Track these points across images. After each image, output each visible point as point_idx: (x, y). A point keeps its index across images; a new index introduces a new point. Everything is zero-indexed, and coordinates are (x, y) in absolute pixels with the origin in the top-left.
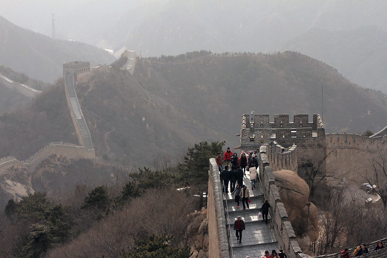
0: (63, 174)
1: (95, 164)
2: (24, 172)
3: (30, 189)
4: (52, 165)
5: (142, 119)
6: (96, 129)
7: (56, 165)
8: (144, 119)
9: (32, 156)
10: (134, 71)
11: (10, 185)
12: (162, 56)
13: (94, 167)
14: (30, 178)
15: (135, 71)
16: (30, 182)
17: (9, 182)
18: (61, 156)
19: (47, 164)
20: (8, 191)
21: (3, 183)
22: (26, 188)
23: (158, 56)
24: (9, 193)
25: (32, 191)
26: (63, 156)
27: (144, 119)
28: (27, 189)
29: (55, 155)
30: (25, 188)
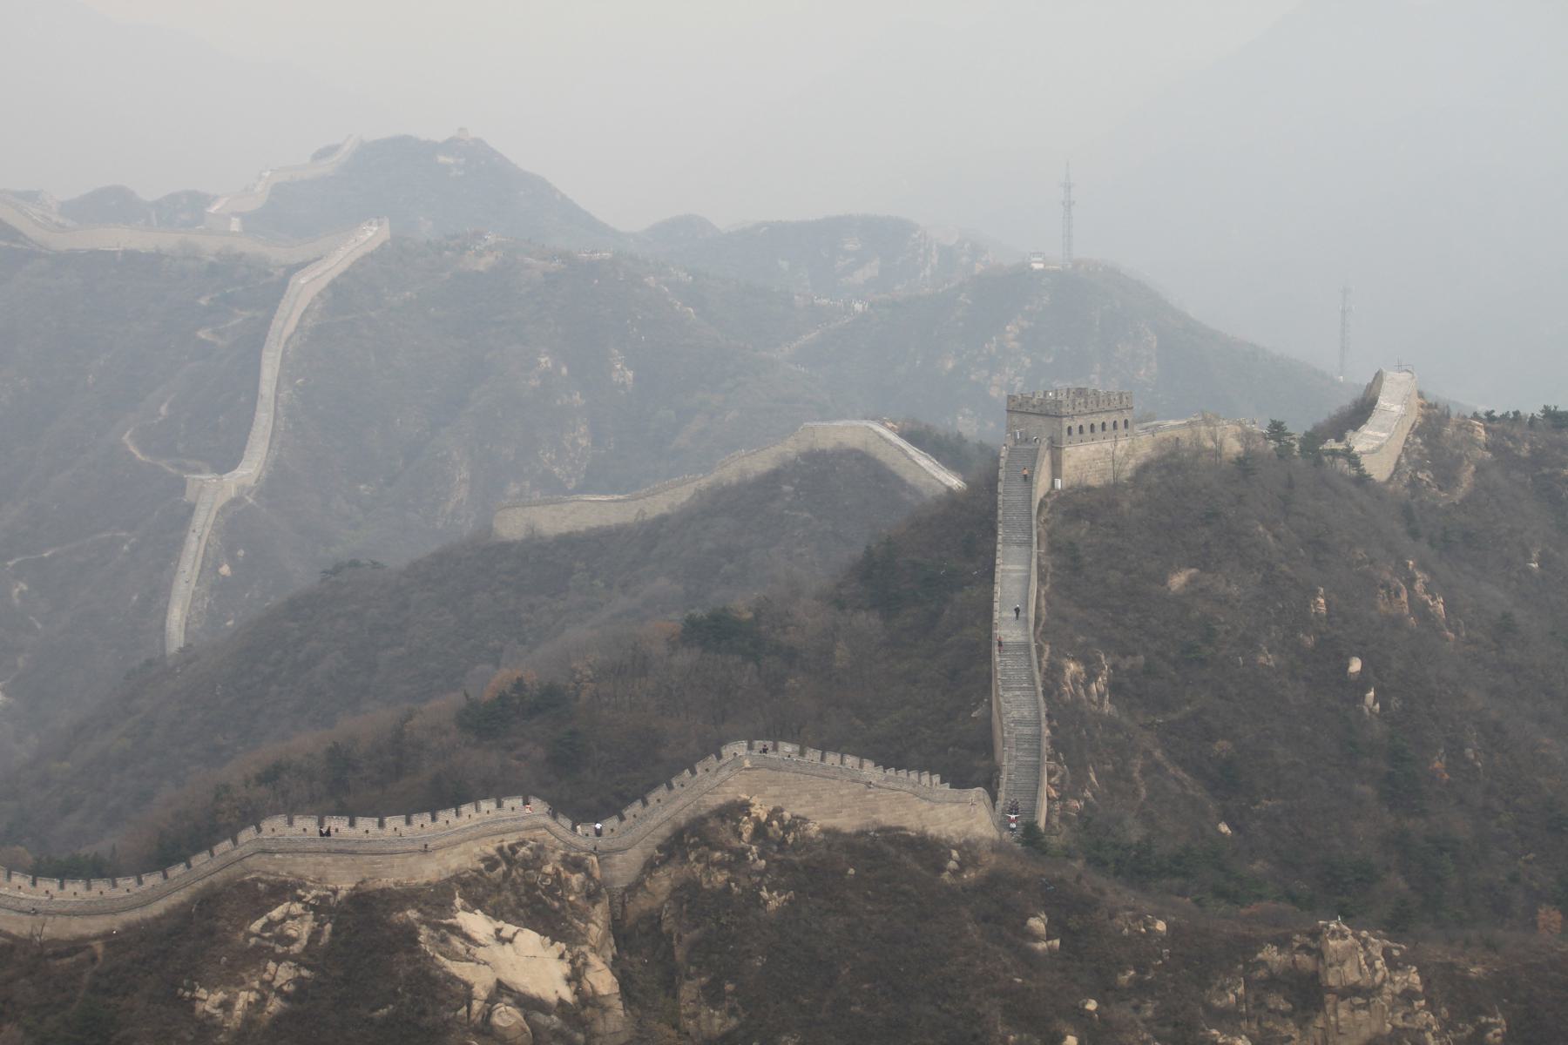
0: (766, 902)
1: (952, 865)
2: (567, 879)
3: (586, 964)
4: (718, 855)
5: (1348, 665)
6: (1101, 696)
7: (741, 854)
8: (1356, 666)
9: (638, 803)
10: (1398, 463)
11: (476, 936)
12: (1546, 410)
13: (946, 876)
14: (600, 913)
15: (1400, 457)
16: (596, 931)
17: (477, 924)
18: (776, 813)
19: (695, 846)
20: (455, 968)
21: (436, 927)
22: (568, 956)
23: (1532, 408)
24: (453, 979)
26: (787, 815)
27: (1356, 666)
28: (572, 962)
29: (744, 807)
30: (562, 957)
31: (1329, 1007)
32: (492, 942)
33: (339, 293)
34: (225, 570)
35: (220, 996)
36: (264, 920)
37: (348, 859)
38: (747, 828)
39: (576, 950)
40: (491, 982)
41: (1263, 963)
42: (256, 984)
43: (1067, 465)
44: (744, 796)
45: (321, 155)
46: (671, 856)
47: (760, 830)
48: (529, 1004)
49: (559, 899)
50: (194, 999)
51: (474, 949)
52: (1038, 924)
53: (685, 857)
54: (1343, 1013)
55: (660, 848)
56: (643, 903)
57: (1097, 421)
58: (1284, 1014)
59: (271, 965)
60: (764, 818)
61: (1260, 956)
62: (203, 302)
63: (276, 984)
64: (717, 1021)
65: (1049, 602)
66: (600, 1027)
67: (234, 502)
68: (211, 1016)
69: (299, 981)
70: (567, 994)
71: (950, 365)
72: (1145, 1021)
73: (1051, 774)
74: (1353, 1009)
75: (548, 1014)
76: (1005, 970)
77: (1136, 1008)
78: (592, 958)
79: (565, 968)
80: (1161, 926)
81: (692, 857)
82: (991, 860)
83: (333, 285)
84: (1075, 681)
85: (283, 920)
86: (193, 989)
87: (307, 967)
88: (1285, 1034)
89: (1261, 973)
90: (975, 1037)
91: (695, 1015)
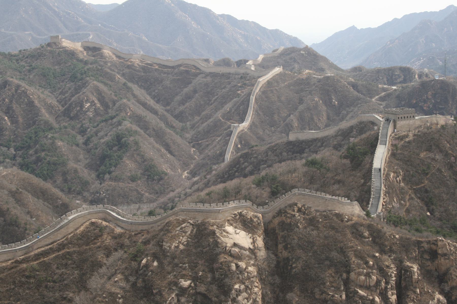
11: (230, 232)
17: (230, 229)
18: (304, 206)
22: (252, 237)
25: (260, 242)
26: (306, 206)
28: (253, 239)
29: (296, 204)
30: (250, 238)
31: (439, 259)
32: (234, 234)
33: (269, 83)
34: (239, 146)
35: (168, 244)
36: (180, 227)
37: (201, 213)
38: (296, 209)
39: (254, 236)
40: (233, 243)
41: (423, 247)
42: (177, 242)
43: (398, 126)
44: (296, 202)
45: (274, 51)
46: (278, 215)
48: (241, 248)
49: (251, 224)
50: (162, 245)
51: (229, 235)
53: (282, 215)
54: (442, 260)
55: (276, 213)
56: (272, 226)
57: (406, 116)
58: (427, 260)
59: (181, 238)
60: (300, 207)
61: (422, 245)
62: (239, 85)
63: (182, 242)
64: (286, 254)
65: (389, 158)
66: (258, 255)
67: (242, 130)
68: (166, 249)
70: (251, 247)
71: (414, 102)
72: (391, 259)
73: (384, 199)
74: (445, 259)
75: (246, 251)
76: (356, 245)
77: (390, 256)
78: (258, 238)
79: (251, 240)
81: (283, 215)
82: (355, 219)
83: (268, 81)
84: (393, 177)
85: (185, 227)
86: (162, 243)
87: (190, 238)
88: (428, 264)
89: (422, 249)
90: (347, 261)
91: (281, 253)
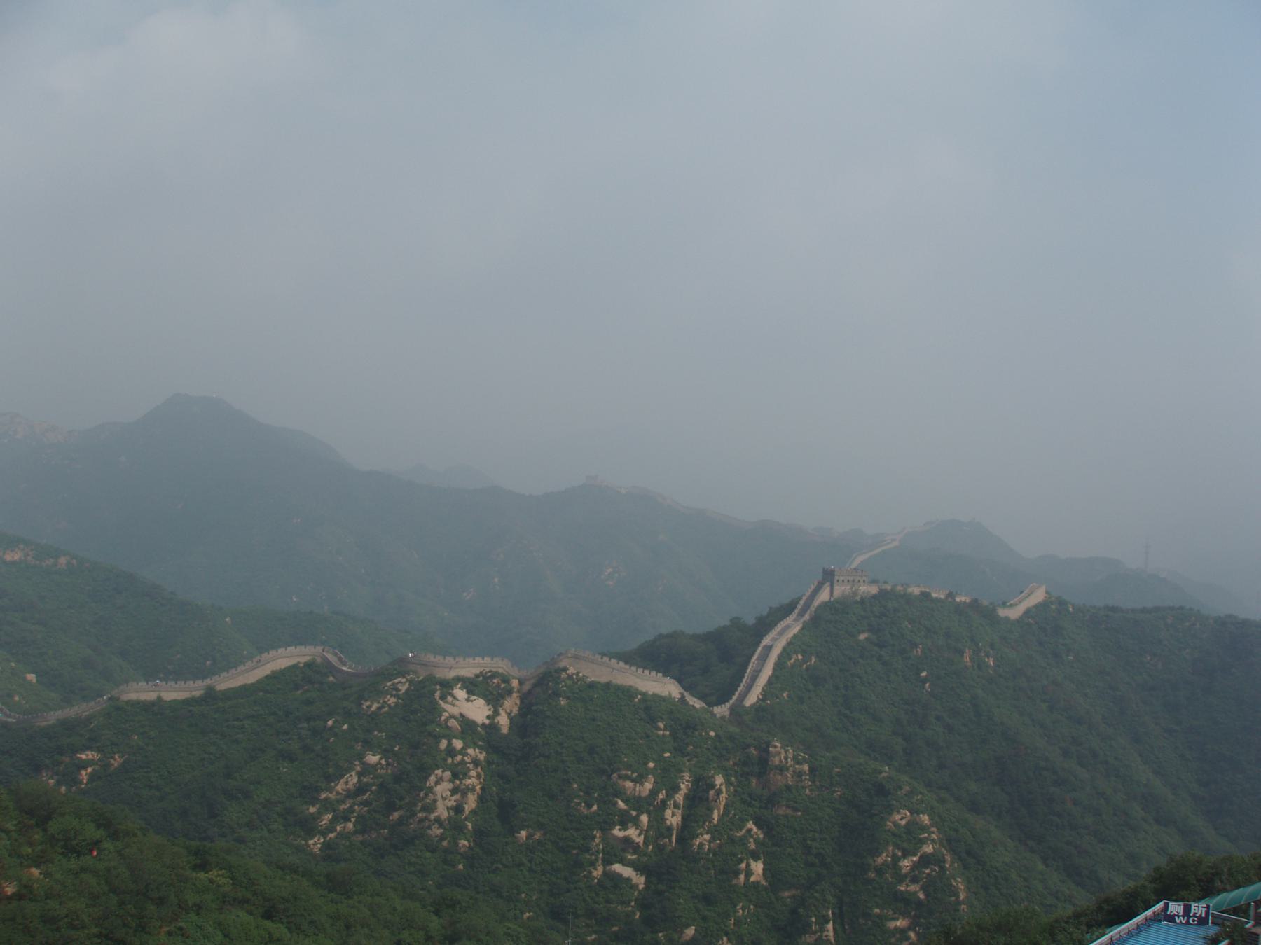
17: (461, 694)
18: (578, 674)
47: (570, 677)
52: (661, 725)
69: (396, 704)
70: (487, 722)
80: (712, 734)
